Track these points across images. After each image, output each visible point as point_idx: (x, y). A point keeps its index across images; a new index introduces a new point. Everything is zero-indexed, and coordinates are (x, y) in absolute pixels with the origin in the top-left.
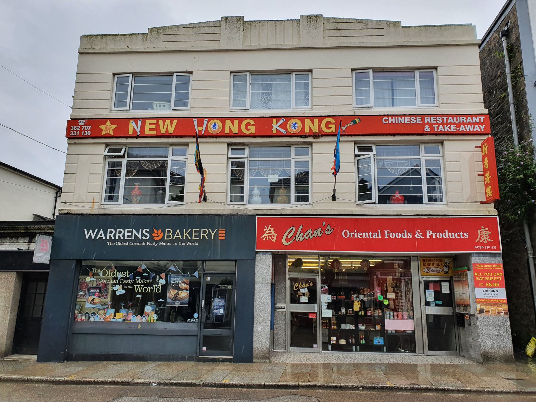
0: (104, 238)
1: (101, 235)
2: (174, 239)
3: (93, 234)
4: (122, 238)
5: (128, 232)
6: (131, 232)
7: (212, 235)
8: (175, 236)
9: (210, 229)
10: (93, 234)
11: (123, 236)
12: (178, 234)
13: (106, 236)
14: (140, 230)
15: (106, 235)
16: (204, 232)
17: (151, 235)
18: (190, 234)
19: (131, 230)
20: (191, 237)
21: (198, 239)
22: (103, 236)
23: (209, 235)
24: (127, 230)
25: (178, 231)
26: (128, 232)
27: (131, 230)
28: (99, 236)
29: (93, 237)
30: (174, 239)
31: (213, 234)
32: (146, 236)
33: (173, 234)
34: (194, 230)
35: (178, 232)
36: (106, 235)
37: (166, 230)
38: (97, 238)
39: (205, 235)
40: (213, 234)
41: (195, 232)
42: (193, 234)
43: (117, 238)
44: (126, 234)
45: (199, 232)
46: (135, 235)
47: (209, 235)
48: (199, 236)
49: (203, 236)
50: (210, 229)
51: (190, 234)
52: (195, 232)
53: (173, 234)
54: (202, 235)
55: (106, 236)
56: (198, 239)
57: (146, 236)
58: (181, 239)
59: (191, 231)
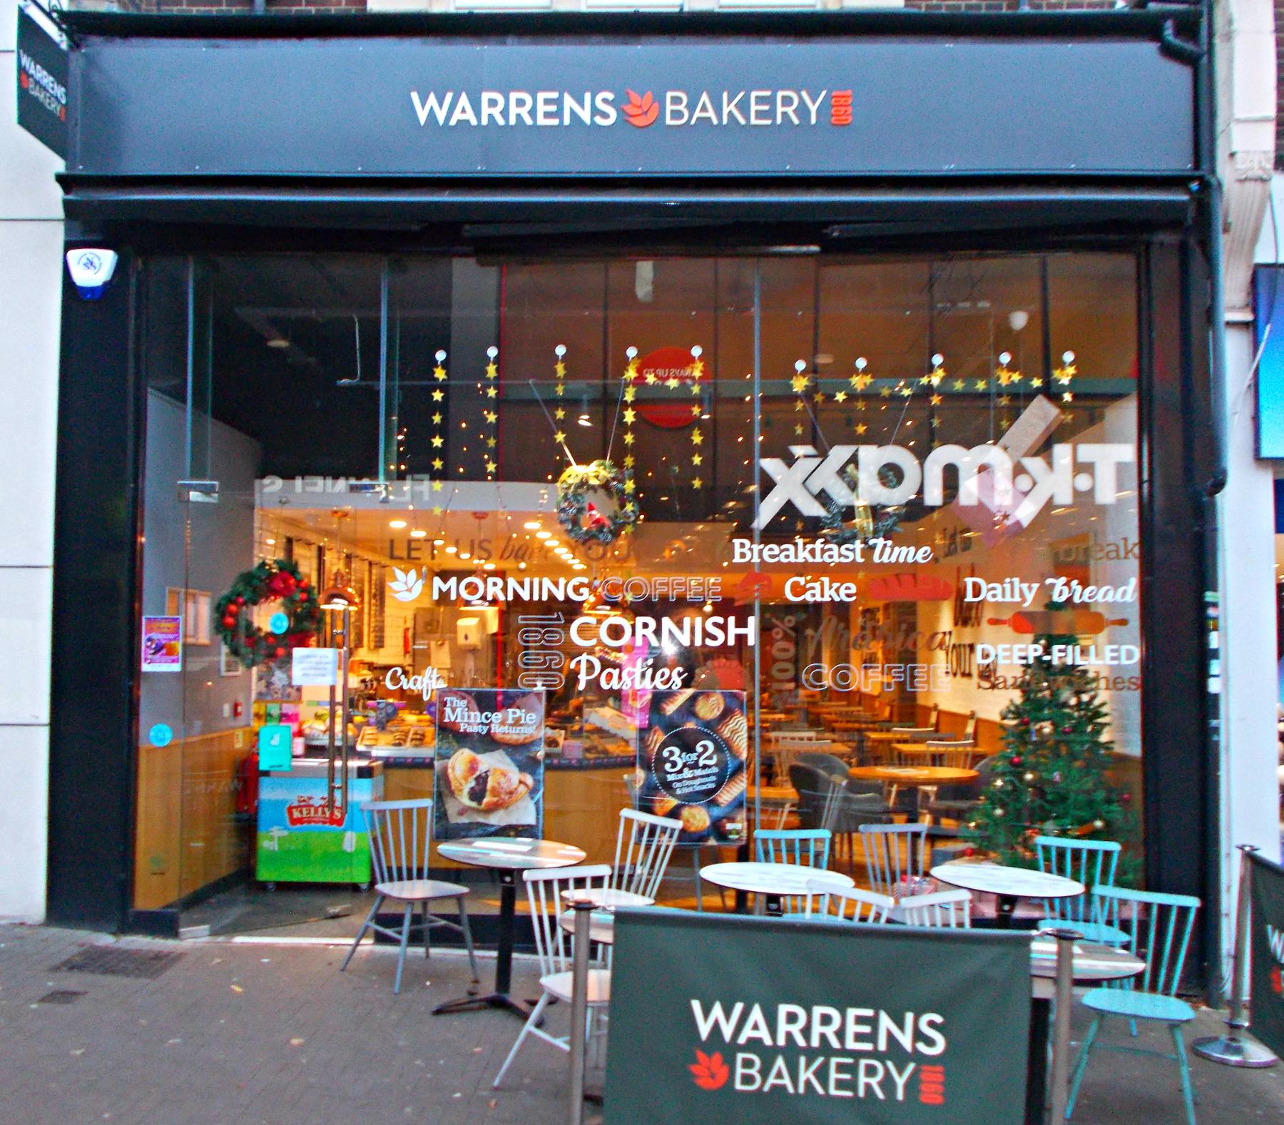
0: (474, 122)
1: (464, 112)
2: (693, 122)
3: (441, 106)
4: (529, 121)
5: (547, 102)
6: (559, 102)
7: (809, 112)
8: (697, 114)
9: (804, 94)
10: (441, 106)
11: (533, 113)
12: (704, 109)
13: (478, 114)
14: (588, 96)
15: (478, 112)
16: (787, 101)
17: (620, 111)
18: (744, 107)
19: (555, 95)
20: (747, 118)
21: (768, 122)
22: (470, 116)
23: (803, 111)
24: (541, 96)
25: (705, 98)
26: (547, 102)
27: (555, 95)
28: (457, 116)
29: (441, 116)
30: (693, 122)
31: (813, 109)
32: (605, 116)
33: (691, 107)
34: (754, 94)
35: (704, 104)
36: (478, 112)
37: (669, 95)
38: (453, 122)
39: (790, 110)
40: (813, 109)
41: (760, 100)
42: (754, 108)
43: (512, 121)
44: (542, 108)
45: (771, 101)
46: (572, 112)
47: (803, 111)
48: (771, 114)
49: (784, 114)
50: (804, 94)
51: (744, 107)
52: (760, 100)
53: (691, 107)
54: (780, 109)
55: (478, 114)
56: (768, 122)
57: (605, 116)
58: (715, 122)
59: (746, 100)
